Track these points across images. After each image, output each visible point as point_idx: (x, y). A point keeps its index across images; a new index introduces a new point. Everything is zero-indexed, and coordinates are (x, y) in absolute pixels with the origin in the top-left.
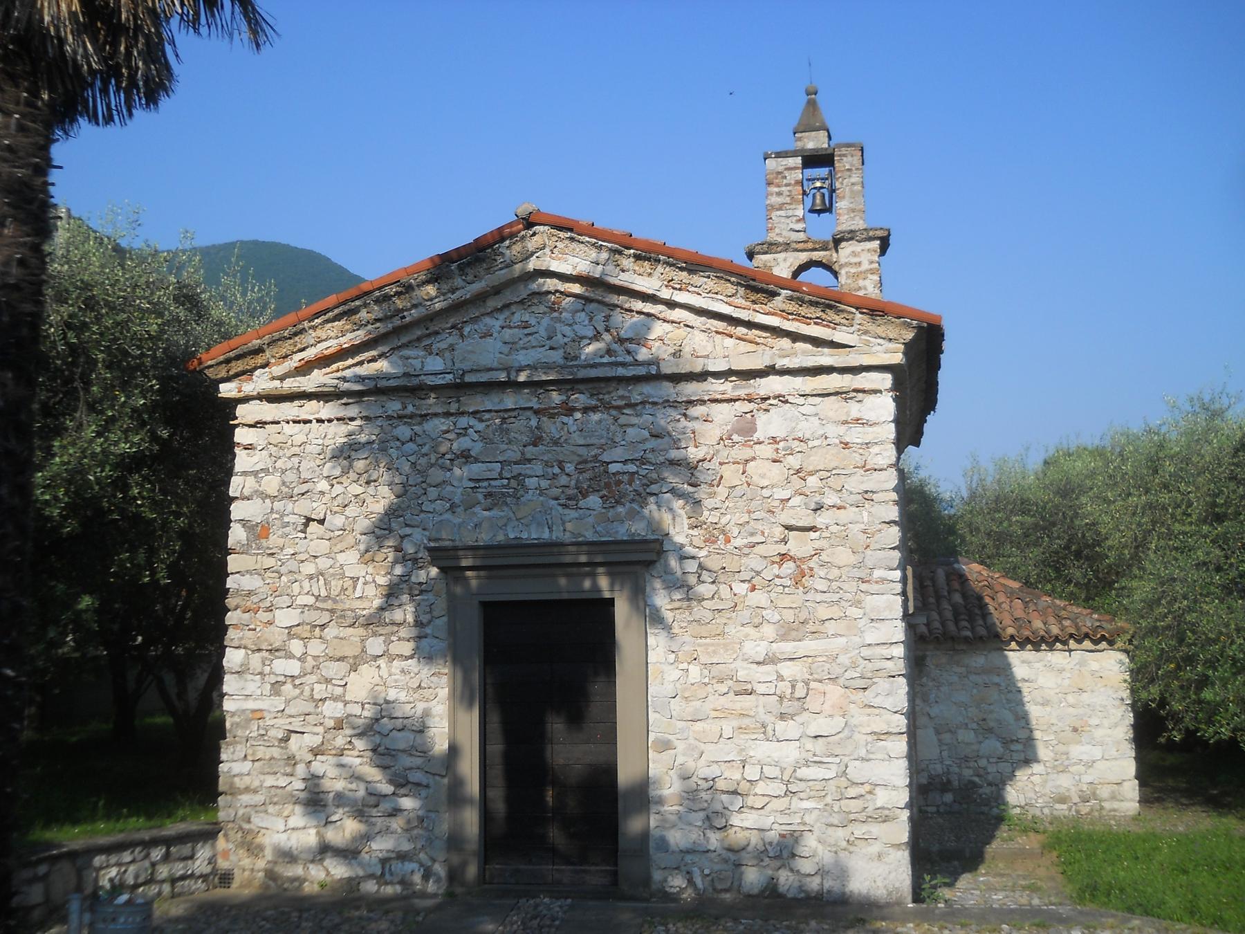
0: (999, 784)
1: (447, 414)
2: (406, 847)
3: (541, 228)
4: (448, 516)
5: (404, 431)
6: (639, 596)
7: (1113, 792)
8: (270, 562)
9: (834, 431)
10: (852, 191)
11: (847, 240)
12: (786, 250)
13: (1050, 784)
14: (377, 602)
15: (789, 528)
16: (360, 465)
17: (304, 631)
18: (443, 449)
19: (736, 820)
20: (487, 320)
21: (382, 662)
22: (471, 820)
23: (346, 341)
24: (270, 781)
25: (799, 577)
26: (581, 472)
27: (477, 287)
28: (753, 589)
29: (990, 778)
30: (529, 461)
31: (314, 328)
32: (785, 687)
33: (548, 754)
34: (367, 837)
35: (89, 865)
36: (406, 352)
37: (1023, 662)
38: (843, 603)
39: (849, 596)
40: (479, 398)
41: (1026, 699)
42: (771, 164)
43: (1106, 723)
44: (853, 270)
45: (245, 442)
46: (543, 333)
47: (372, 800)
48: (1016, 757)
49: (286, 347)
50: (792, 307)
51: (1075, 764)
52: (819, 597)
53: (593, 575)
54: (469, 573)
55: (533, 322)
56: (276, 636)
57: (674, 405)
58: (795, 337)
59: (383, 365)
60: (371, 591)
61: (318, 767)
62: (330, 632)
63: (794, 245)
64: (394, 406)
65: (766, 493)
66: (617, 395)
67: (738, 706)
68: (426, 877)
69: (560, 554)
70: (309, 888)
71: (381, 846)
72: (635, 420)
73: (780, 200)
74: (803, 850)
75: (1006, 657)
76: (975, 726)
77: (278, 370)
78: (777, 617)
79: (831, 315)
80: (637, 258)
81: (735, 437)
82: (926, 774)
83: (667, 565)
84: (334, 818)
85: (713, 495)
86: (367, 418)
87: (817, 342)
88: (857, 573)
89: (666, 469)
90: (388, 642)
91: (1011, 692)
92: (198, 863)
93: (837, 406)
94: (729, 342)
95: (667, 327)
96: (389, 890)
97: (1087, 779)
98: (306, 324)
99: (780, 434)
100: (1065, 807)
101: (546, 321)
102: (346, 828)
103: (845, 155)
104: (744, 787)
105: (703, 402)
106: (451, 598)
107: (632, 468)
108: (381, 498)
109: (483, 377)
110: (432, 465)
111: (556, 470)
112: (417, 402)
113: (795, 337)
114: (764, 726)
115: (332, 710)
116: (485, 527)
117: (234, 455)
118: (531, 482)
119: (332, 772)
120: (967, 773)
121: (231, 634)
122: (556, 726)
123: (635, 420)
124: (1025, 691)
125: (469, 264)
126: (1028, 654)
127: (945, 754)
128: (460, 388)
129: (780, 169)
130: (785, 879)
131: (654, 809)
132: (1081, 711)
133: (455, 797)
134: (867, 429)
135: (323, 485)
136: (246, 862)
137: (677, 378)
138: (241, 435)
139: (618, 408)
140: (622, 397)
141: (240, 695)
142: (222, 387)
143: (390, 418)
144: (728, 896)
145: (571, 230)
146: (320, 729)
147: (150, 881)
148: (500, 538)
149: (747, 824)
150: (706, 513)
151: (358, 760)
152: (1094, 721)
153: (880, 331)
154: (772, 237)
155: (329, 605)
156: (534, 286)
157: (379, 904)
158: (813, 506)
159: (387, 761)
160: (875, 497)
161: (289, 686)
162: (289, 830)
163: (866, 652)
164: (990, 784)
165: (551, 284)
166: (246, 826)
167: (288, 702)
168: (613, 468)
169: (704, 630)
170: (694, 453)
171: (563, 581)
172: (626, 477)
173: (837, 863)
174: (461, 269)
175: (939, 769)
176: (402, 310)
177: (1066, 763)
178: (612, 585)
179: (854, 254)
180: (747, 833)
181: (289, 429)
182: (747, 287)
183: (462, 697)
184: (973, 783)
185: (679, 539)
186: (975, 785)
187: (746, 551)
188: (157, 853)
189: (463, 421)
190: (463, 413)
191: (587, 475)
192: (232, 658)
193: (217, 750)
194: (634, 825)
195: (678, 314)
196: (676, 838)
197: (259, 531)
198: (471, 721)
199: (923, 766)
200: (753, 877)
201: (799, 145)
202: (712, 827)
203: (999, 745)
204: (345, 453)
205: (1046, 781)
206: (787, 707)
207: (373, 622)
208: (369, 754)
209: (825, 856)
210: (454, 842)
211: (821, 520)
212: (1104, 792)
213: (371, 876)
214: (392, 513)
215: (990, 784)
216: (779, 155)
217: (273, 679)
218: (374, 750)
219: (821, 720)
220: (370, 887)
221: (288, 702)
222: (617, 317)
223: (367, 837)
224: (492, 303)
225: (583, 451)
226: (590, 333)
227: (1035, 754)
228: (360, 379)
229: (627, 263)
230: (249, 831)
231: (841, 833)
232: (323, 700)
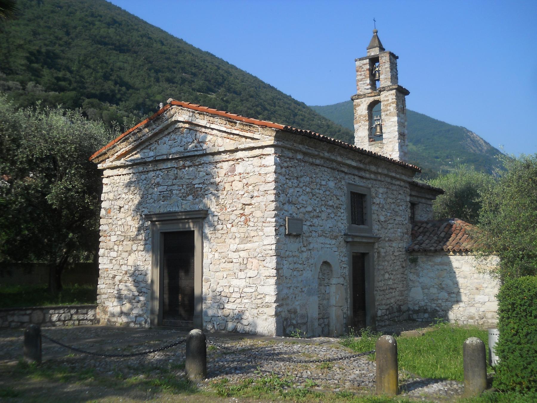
1: (154, 170)
2: (141, 313)
3: (175, 106)
4: (153, 204)
5: (143, 177)
6: (201, 229)
7: (493, 315)
8: (110, 221)
9: (257, 169)
10: (386, 71)
11: (383, 91)
12: (365, 97)
13: (467, 311)
14: (136, 233)
15: (244, 204)
16: (132, 188)
17: (117, 243)
18: (152, 182)
19: (226, 306)
20: (164, 138)
21: (136, 252)
22: (156, 304)
23: (127, 149)
24: (109, 291)
25: (246, 222)
26: (187, 188)
27: (160, 127)
28: (233, 226)
29: (443, 308)
30: (174, 185)
31: (118, 145)
32: (241, 260)
33: (180, 283)
34: (132, 309)
35: (48, 313)
36: (145, 151)
37: (457, 260)
38: (258, 230)
39: (260, 228)
40: (162, 165)
41: (457, 276)
42: (358, 63)
43: (490, 286)
44: (385, 103)
45: (105, 183)
46: (179, 142)
47: (133, 297)
48: (453, 299)
49: (112, 152)
50: (242, 127)
51: (477, 303)
52: (251, 228)
53: (188, 223)
54: (157, 223)
55: (176, 138)
56: (111, 244)
57: (210, 163)
58: (246, 138)
59: (138, 156)
60: (134, 229)
61: (121, 287)
62: (125, 243)
63: (367, 95)
64: (141, 169)
65: (237, 192)
66: (197, 161)
67: (228, 267)
68: (146, 323)
70: (118, 325)
71: (135, 312)
72: (202, 169)
73: (361, 77)
74: (244, 317)
75: (449, 258)
76: (437, 287)
77: (111, 159)
78: (239, 236)
79: (252, 129)
80: (199, 114)
81: (229, 174)
82: (418, 306)
83: (209, 219)
84: (124, 303)
85: (222, 194)
86: (134, 173)
87: (253, 139)
88: (263, 220)
89: (209, 186)
90: (138, 246)
91: (451, 273)
92: (89, 316)
93: (258, 160)
94: (228, 140)
95: (211, 137)
96: (136, 326)
97: (482, 309)
98: (116, 144)
99: (242, 172)
100: (472, 321)
101: (180, 138)
102: (127, 307)
104: (228, 295)
105: (220, 162)
106: (153, 231)
107: (201, 186)
108: (137, 199)
109: (160, 158)
110: (150, 188)
111: (181, 188)
112: (147, 167)
113: (246, 138)
114: (235, 274)
115: (124, 268)
116: (163, 207)
117: (102, 188)
118: (174, 192)
119: (124, 288)
120: (434, 305)
121: (101, 244)
122: (182, 274)
123: (202, 169)
124: (457, 272)
125: (155, 120)
126: (458, 257)
127: (425, 298)
128: (156, 162)
129: (361, 65)
130: (239, 327)
131: (204, 302)
132: (479, 281)
133: (153, 298)
134: (266, 168)
135: (124, 196)
136: (103, 316)
137: (213, 154)
138: (105, 181)
139: (197, 166)
140: (199, 162)
141: (103, 263)
142: (99, 165)
143: (139, 173)
144: (224, 332)
145: (182, 106)
146: (121, 274)
147: (71, 319)
148: (166, 211)
149: (230, 308)
150: (220, 200)
151: (130, 284)
152: (485, 285)
153: (266, 133)
154: (359, 92)
155: (123, 234)
156: (176, 126)
157: (134, 331)
158: (250, 196)
159: (137, 285)
160: (268, 192)
161: (114, 260)
162: (113, 306)
163: (264, 247)
164: (443, 311)
165: (181, 125)
166: (104, 305)
167: (114, 265)
168: (196, 186)
169: (219, 241)
170: (218, 180)
171: (181, 225)
172: (199, 189)
173: (253, 322)
174: (154, 122)
175: (423, 303)
176: (141, 137)
177: (474, 302)
178: (194, 226)
179: (386, 96)
180: (229, 311)
181: (116, 178)
182: (229, 121)
183: (154, 264)
184: (436, 309)
185: (213, 210)
186: (437, 311)
187: (231, 213)
188: (73, 311)
189: (158, 172)
190: (157, 170)
191: (189, 189)
192: (101, 252)
193: (97, 281)
194: (199, 308)
195: (215, 132)
196: (210, 313)
197: (108, 211)
198: (157, 272)
199: (417, 302)
200: (230, 325)
201: (368, 54)
202: (220, 308)
203: (446, 295)
204: (128, 185)
205: (465, 310)
206: (243, 267)
207: (134, 239)
208: (133, 282)
209: (250, 319)
210: (152, 312)
211: (253, 202)
213: (132, 321)
214: (140, 203)
215: (443, 311)
216: (360, 59)
217: (110, 258)
218: (134, 281)
219: (251, 271)
220: (132, 325)
221: (114, 265)
222: (198, 134)
223: (132, 309)
224: (166, 133)
225: (188, 181)
226: (191, 141)
227: (460, 298)
228: (131, 161)
229: (197, 116)
230: (104, 307)
231: (256, 311)
232: (122, 265)
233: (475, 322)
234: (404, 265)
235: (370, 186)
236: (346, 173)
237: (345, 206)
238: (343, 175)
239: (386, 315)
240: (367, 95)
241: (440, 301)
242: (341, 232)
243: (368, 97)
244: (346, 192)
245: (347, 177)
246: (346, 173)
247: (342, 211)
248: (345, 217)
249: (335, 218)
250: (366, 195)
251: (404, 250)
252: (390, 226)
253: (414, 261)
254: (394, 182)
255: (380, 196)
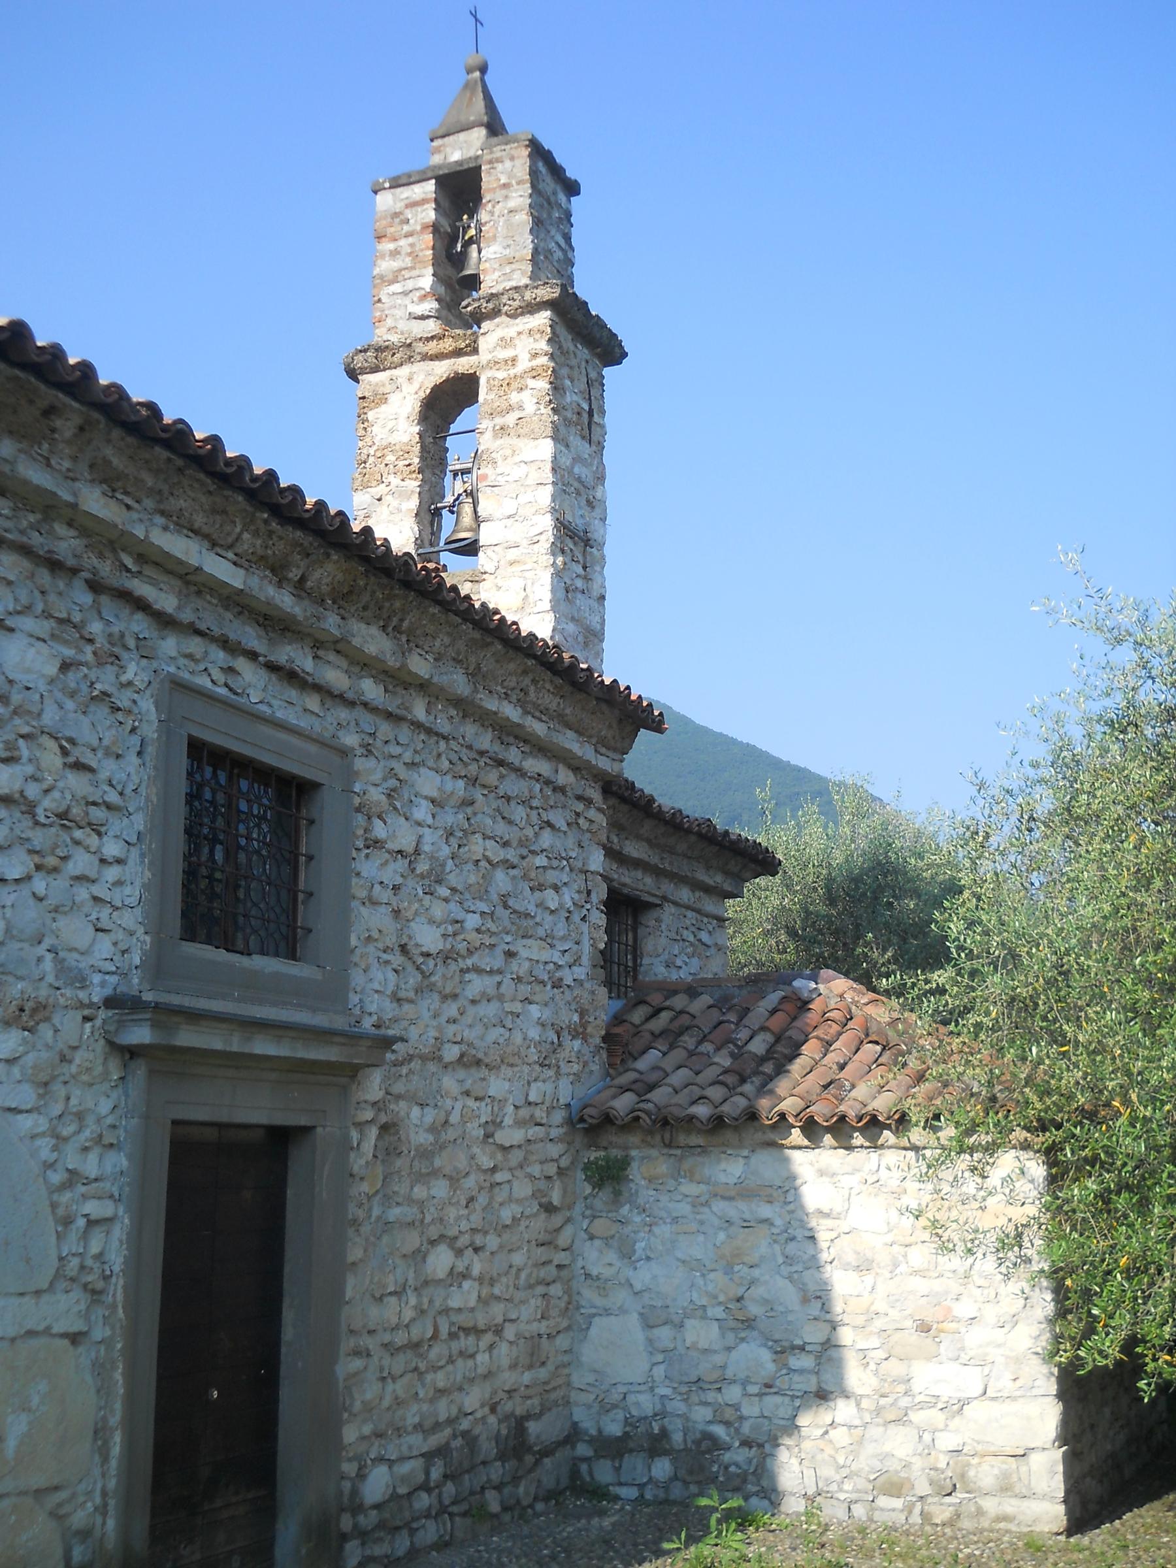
0: (764, 1445)
7: (1006, 1475)
10: (509, 225)
12: (410, 359)
13: (870, 1449)
29: (746, 1428)
37: (821, 1173)
41: (824, 1256)
42: (386, 201)
44: (501, 375)
51: (921, 1406)
63: (420, 347)
73: (396, 264)
76: (719, 1312)
82: (620, 1415)
91: (796, 1239)
97: (947, 1441)
100: (898, 1503)
103: (499, 160)
120: (701, 1415)
124: (823, 1237)
127: (659, 1372)
129: (399, 206)
132: (937, 1285)
152: (964, 1309)
154: (382, 335)
164: (746, 1443)
175: (644, 1404)
177: (904, 1402)
179: (505, 343)
199: (615, 1397)
201: (437, 159)
203: (766, 1356)
205: (861, 1441)
212: (985, 1474)
215: (746, 1443)
216: (397, 183)
227: (840, 1378)
233: (909, 1509)
234: (556, 1198)
235: (350, 740)
236: (165, 621)
237: (139, 822)
238: (139, 624)
239: (425, 1487)
240: (420, 347)
241: (733, 1393)
242: (82, 982)
243: (427, 357)
244: (150, 730)
245: (170, 645)
246: (165, 621)
247: (112, 849)
248: (131, 893)
249: (40, 884)
250: (315, 786)
251: (559, 1116)
252: (477, 985)
253: (610, 1176)
254: (513, 755)
255: (422, 812)
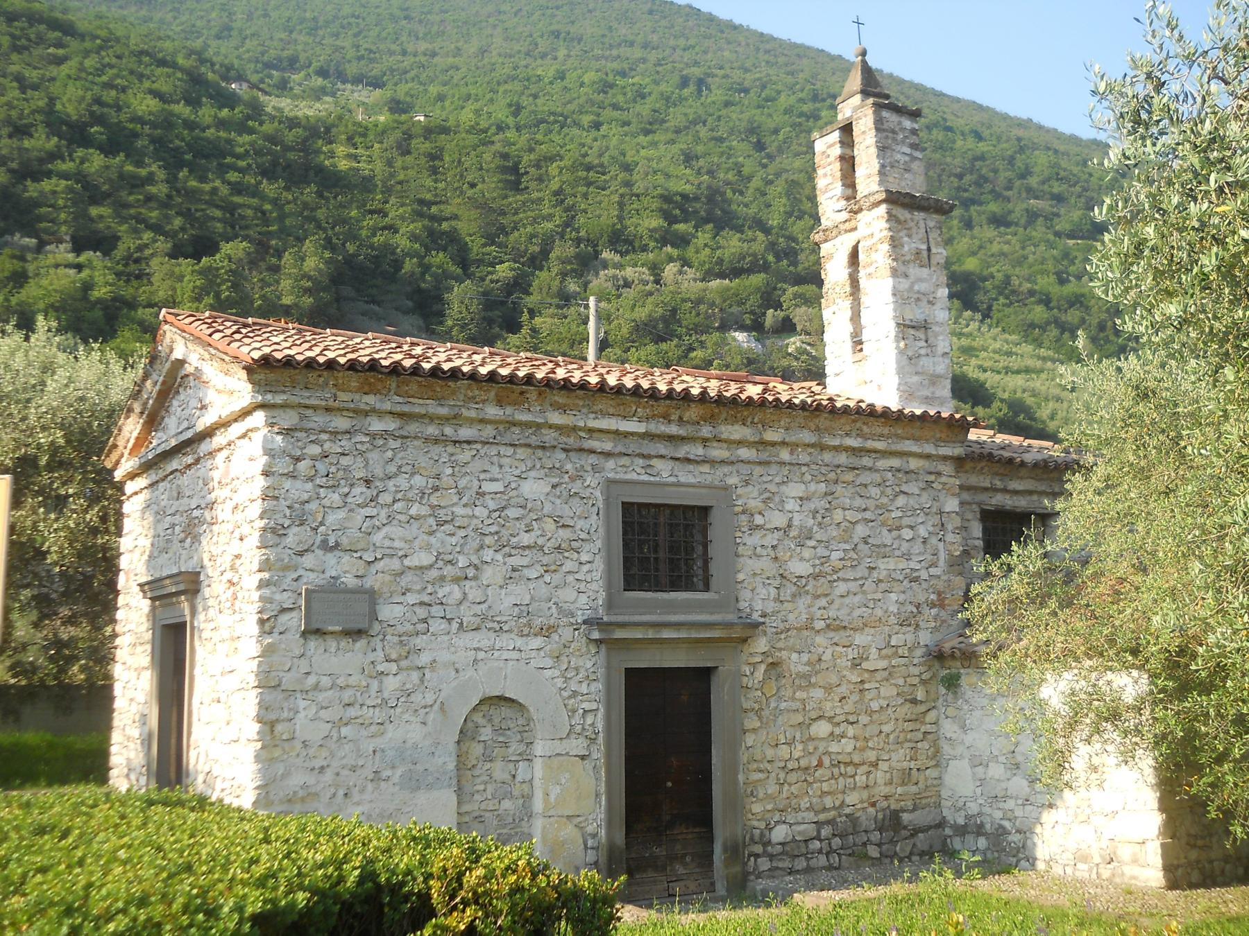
0: (1026, 832)
63: (842, 227)
69: (164, 587)
82: (963, 813)
103: (860, 118)
120: (998, 815)
127: (979, 791)
164: (1019, 831)
175: (973, 808)
203: (1025, 783)
212: (1125, 853)
215: (1019, 831)
233: (1090, 870)
234: (920, 695)
235: (732, 480)
236: (608, 455)
237: (599, 544)
238: (592, 459)
239: (818, 838)
240: (842, 227)
241: (1010, 804)
243: (846, 231)
244: (600, 504)
245: (611, 464)
246: (608, 455)
247: (585, 557)
248: (597, 575)
249: (547, 578)
250: (705, 511)
251: (919, 652)
252: (842, 588)
253: (952, 683)
254: (866, 461)
255: (791, 505)
